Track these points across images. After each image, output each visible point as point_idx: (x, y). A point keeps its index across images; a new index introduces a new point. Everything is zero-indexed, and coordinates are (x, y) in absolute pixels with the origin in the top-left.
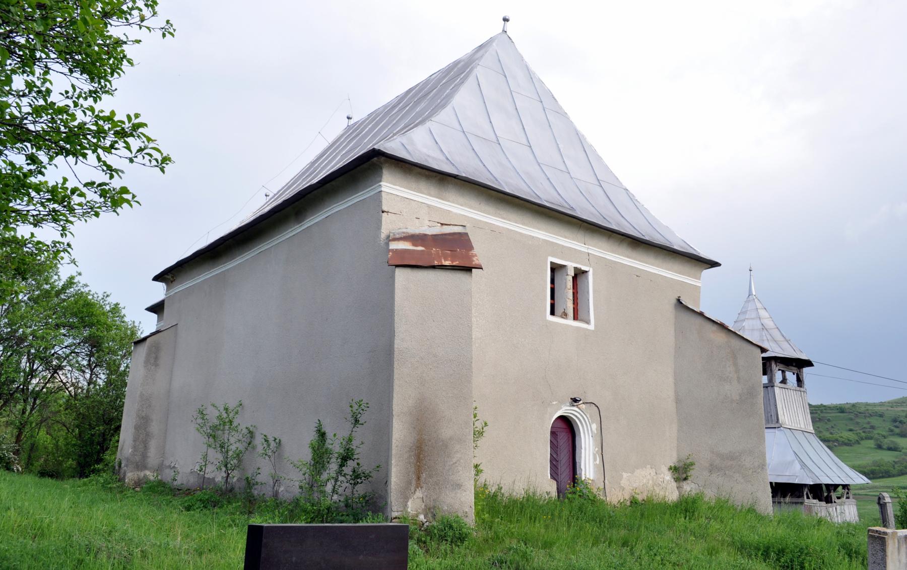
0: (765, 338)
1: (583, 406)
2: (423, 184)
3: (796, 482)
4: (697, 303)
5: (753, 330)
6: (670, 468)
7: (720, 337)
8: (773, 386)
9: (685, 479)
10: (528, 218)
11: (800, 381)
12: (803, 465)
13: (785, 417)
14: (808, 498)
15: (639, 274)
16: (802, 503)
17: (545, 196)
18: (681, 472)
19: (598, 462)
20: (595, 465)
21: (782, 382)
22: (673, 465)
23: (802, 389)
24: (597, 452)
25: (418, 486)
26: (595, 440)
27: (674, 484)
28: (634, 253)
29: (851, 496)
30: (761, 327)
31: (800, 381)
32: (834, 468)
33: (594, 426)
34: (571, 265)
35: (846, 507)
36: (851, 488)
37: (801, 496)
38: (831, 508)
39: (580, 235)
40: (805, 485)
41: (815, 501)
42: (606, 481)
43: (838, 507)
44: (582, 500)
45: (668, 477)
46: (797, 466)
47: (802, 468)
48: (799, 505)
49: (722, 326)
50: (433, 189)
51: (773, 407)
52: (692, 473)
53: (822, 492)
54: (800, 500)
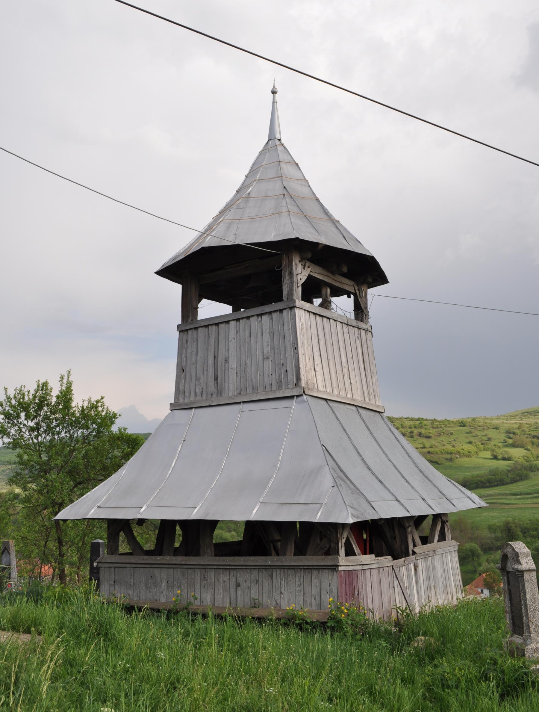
0: (284, 209)
3: (318, 517)
5: (265, 198)
8: (292, 308)
11: (360, 310)
12: (341, 477)
13: (315, 373)
14: (349, 552)
16: (334, 568)
21: (321, 305)
23: (362, 325)
29: (448, 534)
30: (282, 191)
31: (360, 310)
32: (416, 480)
35: (437, 558)
36: (451, 519)
37: (333, 551)
38: (405, 568)
40: (344, 525)
41: (369, 558)
43: (420, 563)
46: (327, 480)
47: (335, 485)
48: (325, 574)
51: (290, 353)
53: (386, 537)
54: (328, 561)
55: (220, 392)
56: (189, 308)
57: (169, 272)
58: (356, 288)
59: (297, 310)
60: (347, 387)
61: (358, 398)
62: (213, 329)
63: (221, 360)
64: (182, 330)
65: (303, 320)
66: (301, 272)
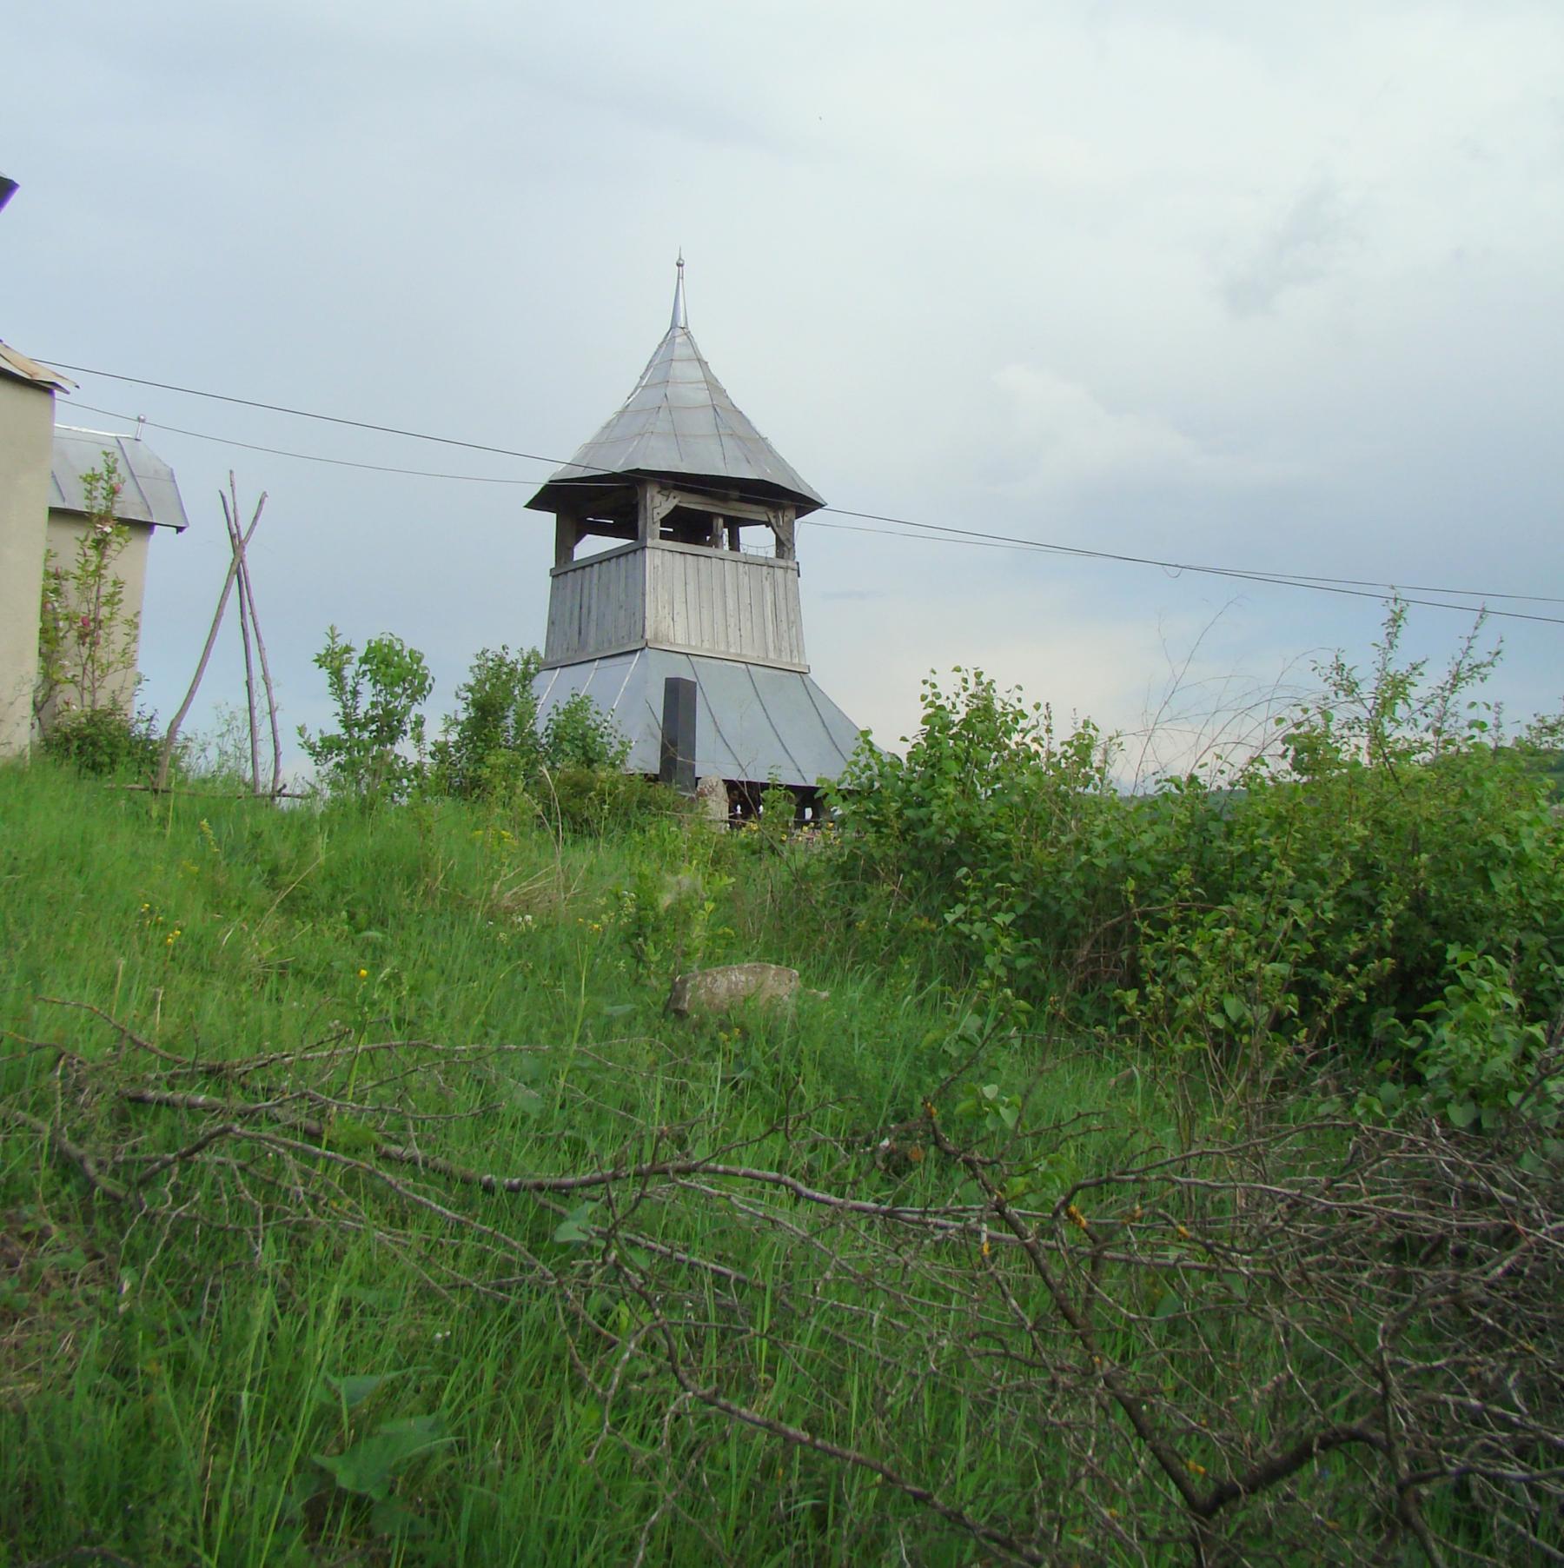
31: (784, 546)
51: (639, 602)
55: (582, 645)
56: (564, 547)
57: (543, 501)
58: (771, 515)
59: (648, 552)
60: (731, 639)
61: (751, 654)
62: (579, 572)
63: (585, 610)
64: (555, 575)
65: (658, 562)
66: (659, 505)
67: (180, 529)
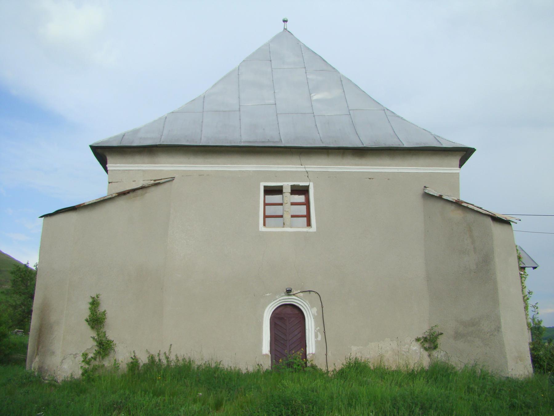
1: (301, 294)
2: (138, 158)
4: (456, 187)
6: (418, 340)
7: (456, 214)
9: (435, 347)
10: (236, 158)
15: (371, 177)
17: (244, 138)
18: (430, 342)
19: (319, 338)
20: (317, 342)
22: (420, 336)
24: (319, 330)
25: (37, 354)
26: (316, 322)
27: (426, 354)
28: (363, 161)
33: (315, 310)
34: (287, 185)
39: (296, 159)
42: (329, 354)
44: (302, 368)
45: (416, 347)
49: (458, 204)
50: (146, 159)
52: (441, 341)
67: (534, 268)
